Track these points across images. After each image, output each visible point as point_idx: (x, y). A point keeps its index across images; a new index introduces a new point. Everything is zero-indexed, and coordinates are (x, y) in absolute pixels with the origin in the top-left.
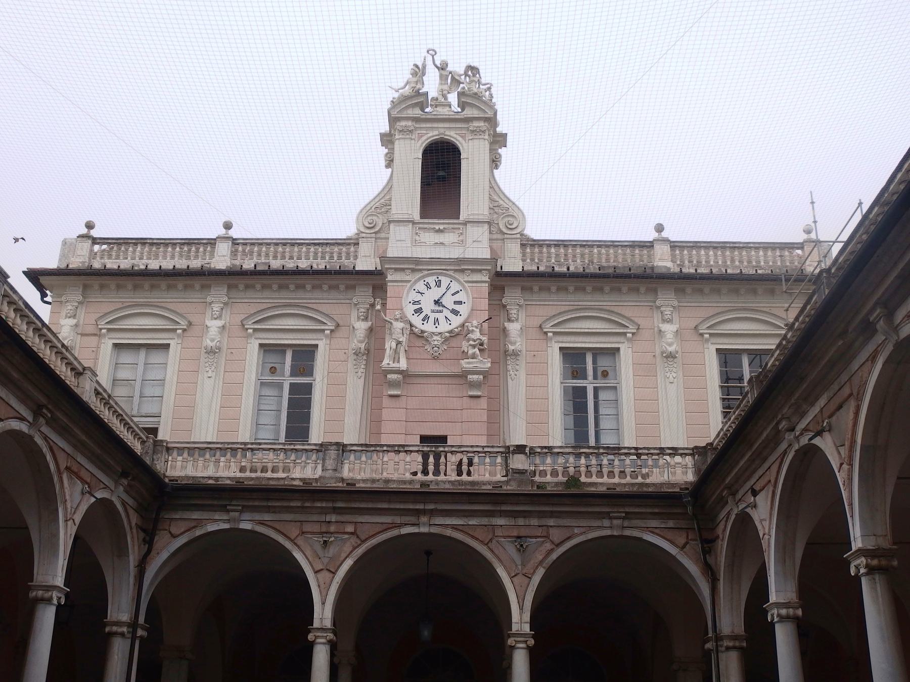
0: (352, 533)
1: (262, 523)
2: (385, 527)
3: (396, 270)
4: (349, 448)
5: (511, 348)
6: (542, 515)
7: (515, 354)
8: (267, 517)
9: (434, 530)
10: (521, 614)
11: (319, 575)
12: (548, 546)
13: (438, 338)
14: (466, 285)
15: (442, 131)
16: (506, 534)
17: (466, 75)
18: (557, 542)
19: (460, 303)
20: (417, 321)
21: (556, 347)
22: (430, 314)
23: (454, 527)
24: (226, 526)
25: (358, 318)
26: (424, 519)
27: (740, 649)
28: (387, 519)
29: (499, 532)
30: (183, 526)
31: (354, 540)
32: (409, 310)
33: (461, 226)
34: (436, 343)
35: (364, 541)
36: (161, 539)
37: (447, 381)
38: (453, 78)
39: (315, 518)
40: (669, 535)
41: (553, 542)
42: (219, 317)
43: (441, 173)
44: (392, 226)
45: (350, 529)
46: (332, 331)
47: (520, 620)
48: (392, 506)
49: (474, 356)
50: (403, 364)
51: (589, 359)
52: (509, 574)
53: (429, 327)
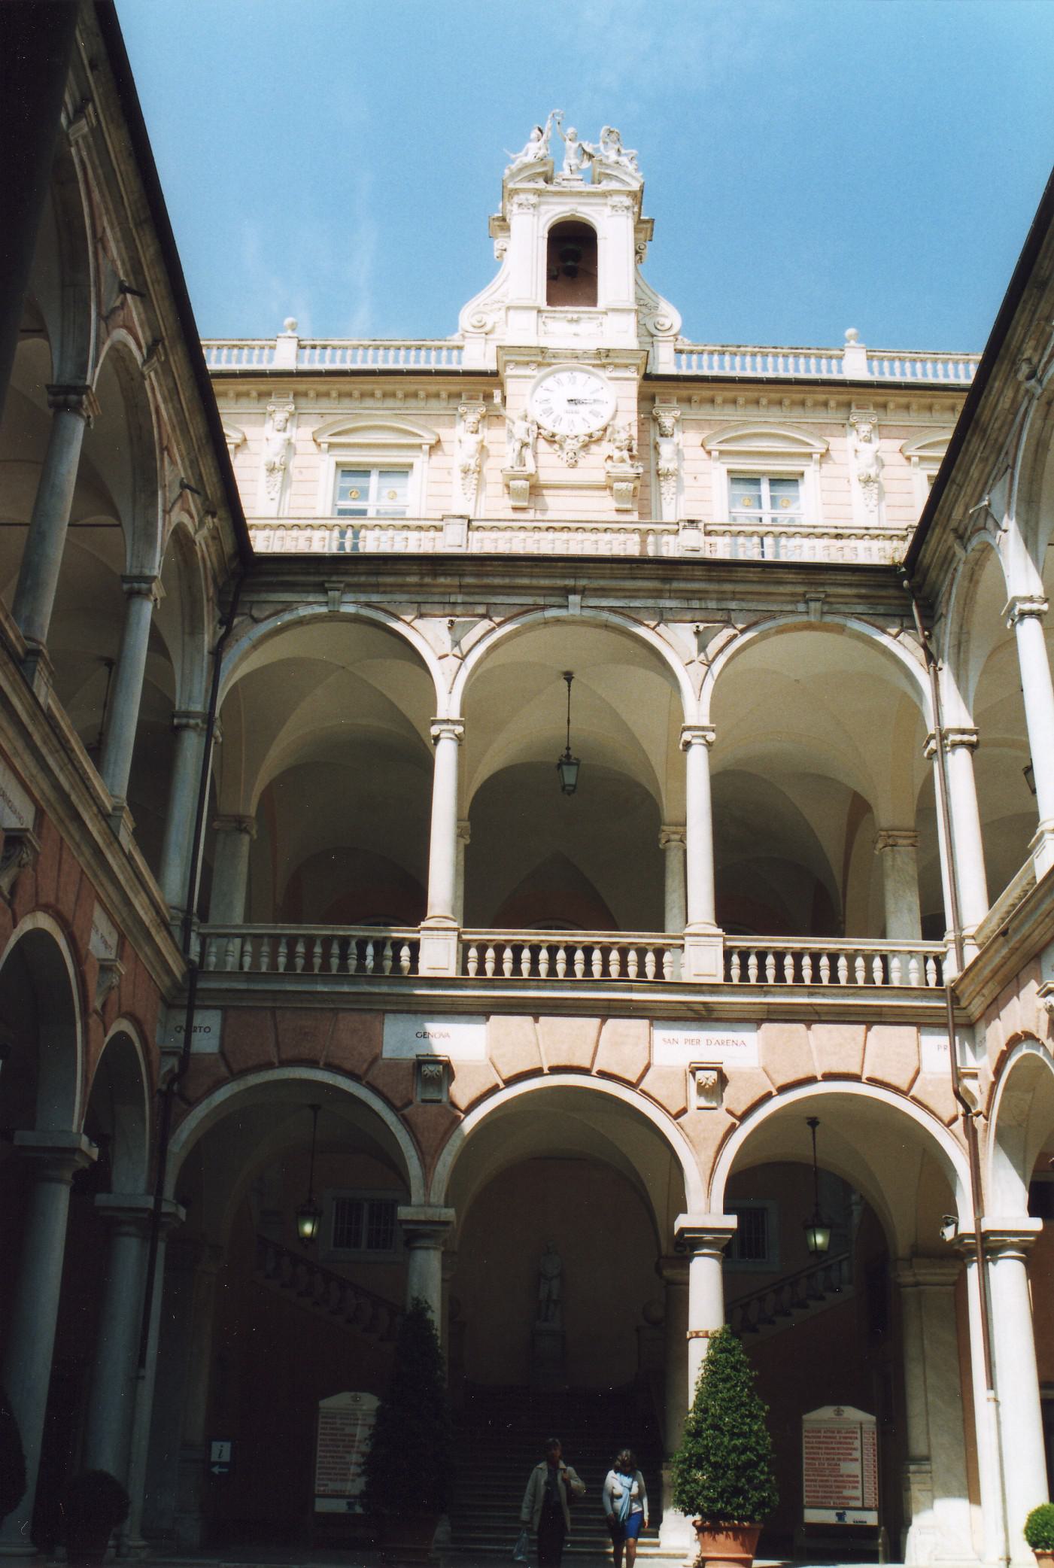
1: (368, 605)
2: (525, 608)
3: (517, 363)
4: (475, 524)
6: (722, 597)
8: (375, 598)
13: (574, 442)
15: (574, 206)
21: (724, 469)
23: (612, 610)
24: (324, 610)
27: (972, 747)
28: (529, 600)
29: (667, 615)
30: (268, 610)
39: (436, 599)
40: (880, 621)
42: (284, 430)
43: (570, 263)
45: (481, 610)
47: (696, 710)
48: (535, 582)
49: (623, 461)
50: (530, 468)
53: (561, 430)
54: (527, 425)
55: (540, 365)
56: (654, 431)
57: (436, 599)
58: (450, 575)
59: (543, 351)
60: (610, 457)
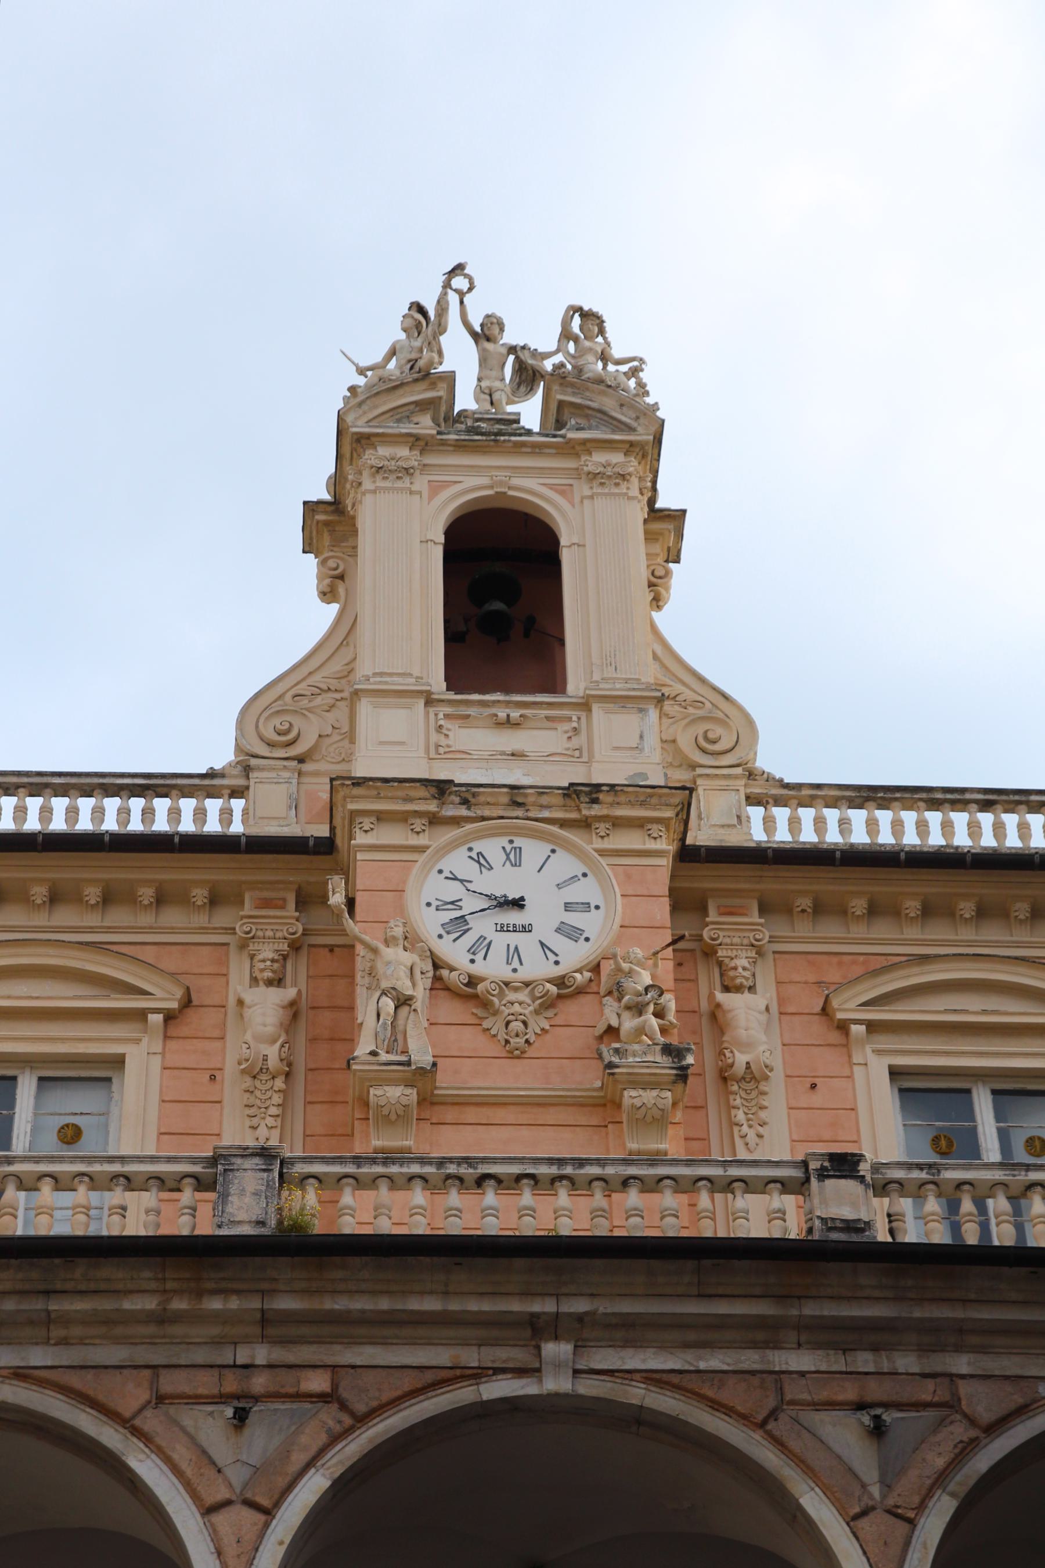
0: (323, 1398)
2: (429, 1377)
3: (381, 817)
4: (301, 1169)
5: (741, 1059)
7: (754, 1077)
8: (38, 1357)
9: (588, 1387)
11: (218, 1518)
12: (959, 1431)
13: (523, 996)
14: (604, 862)
15: (501, 475)
16: (824, 1395)
17: (566, 335)
18: (986, 1414)
19: (586, 907)
20: (455, 952)
21: (878, 1069)
22: (491, 935)
23: (653, 1378)
25: (254, 981)
26: (555, 1350)
31: (329, 1417)
32: (430, 923)
33: (574, 714)
34: (517, 1008)
35: (362, 1419)
37: (552, 1115)
38: (521, 368)
41: (972, 1422)
43: (498, 606)
44: (365, 708)
45: (317, 1383)
46: (170, 1017)
48: (454, 1306)
50: (421, 1054)
51: (983, 1104)
52: (841, 1510)
53: (493, 968)
54: (409, 958)
55: (434, 820)
56: (706, 980)
57: (200, 1356)
58: (238, 1292)
59: (441, 788)
60: (612, 1032)
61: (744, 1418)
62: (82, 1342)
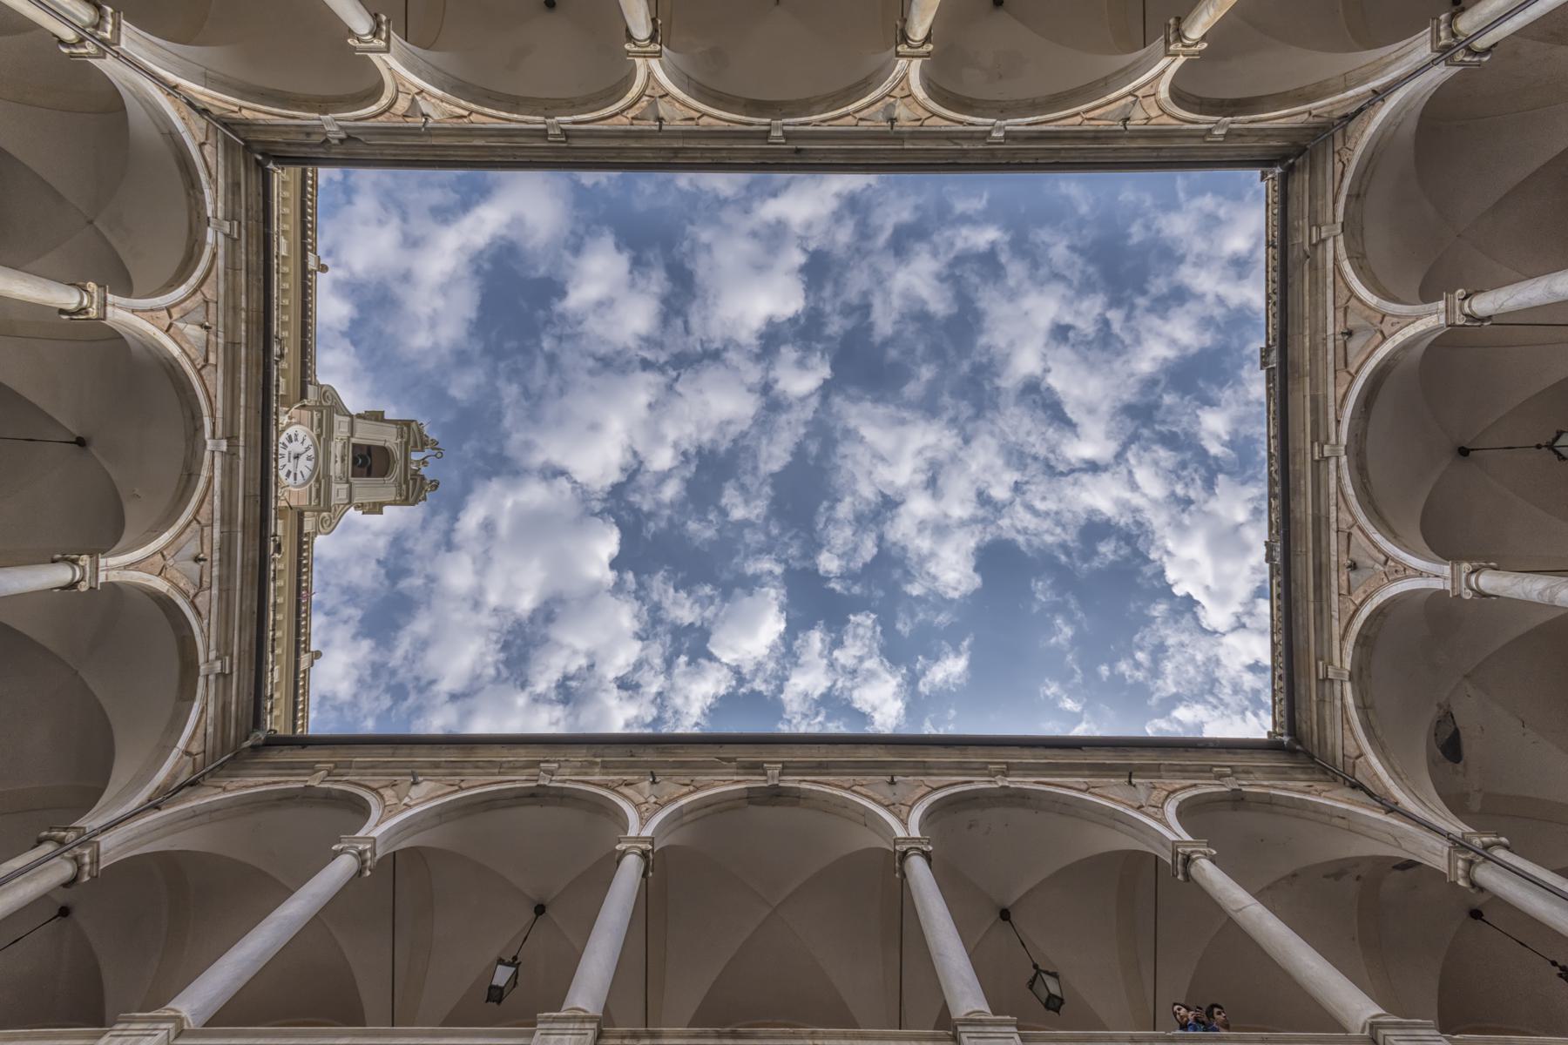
0: (206, 360)
1: (215, 255)
8: (220, 263)
10: (118, 568)
16: (206, 541)
18: (198, 601)
23: (210, 480)
26: (224, 446)
28: (219, 404)
31: (200, 362)
35: (199, 372)
36: (200, 123)
40: (200, 732)
41: (196, 595)
45: (212, 359)
61: (198, 512)
62: (226, 280)
